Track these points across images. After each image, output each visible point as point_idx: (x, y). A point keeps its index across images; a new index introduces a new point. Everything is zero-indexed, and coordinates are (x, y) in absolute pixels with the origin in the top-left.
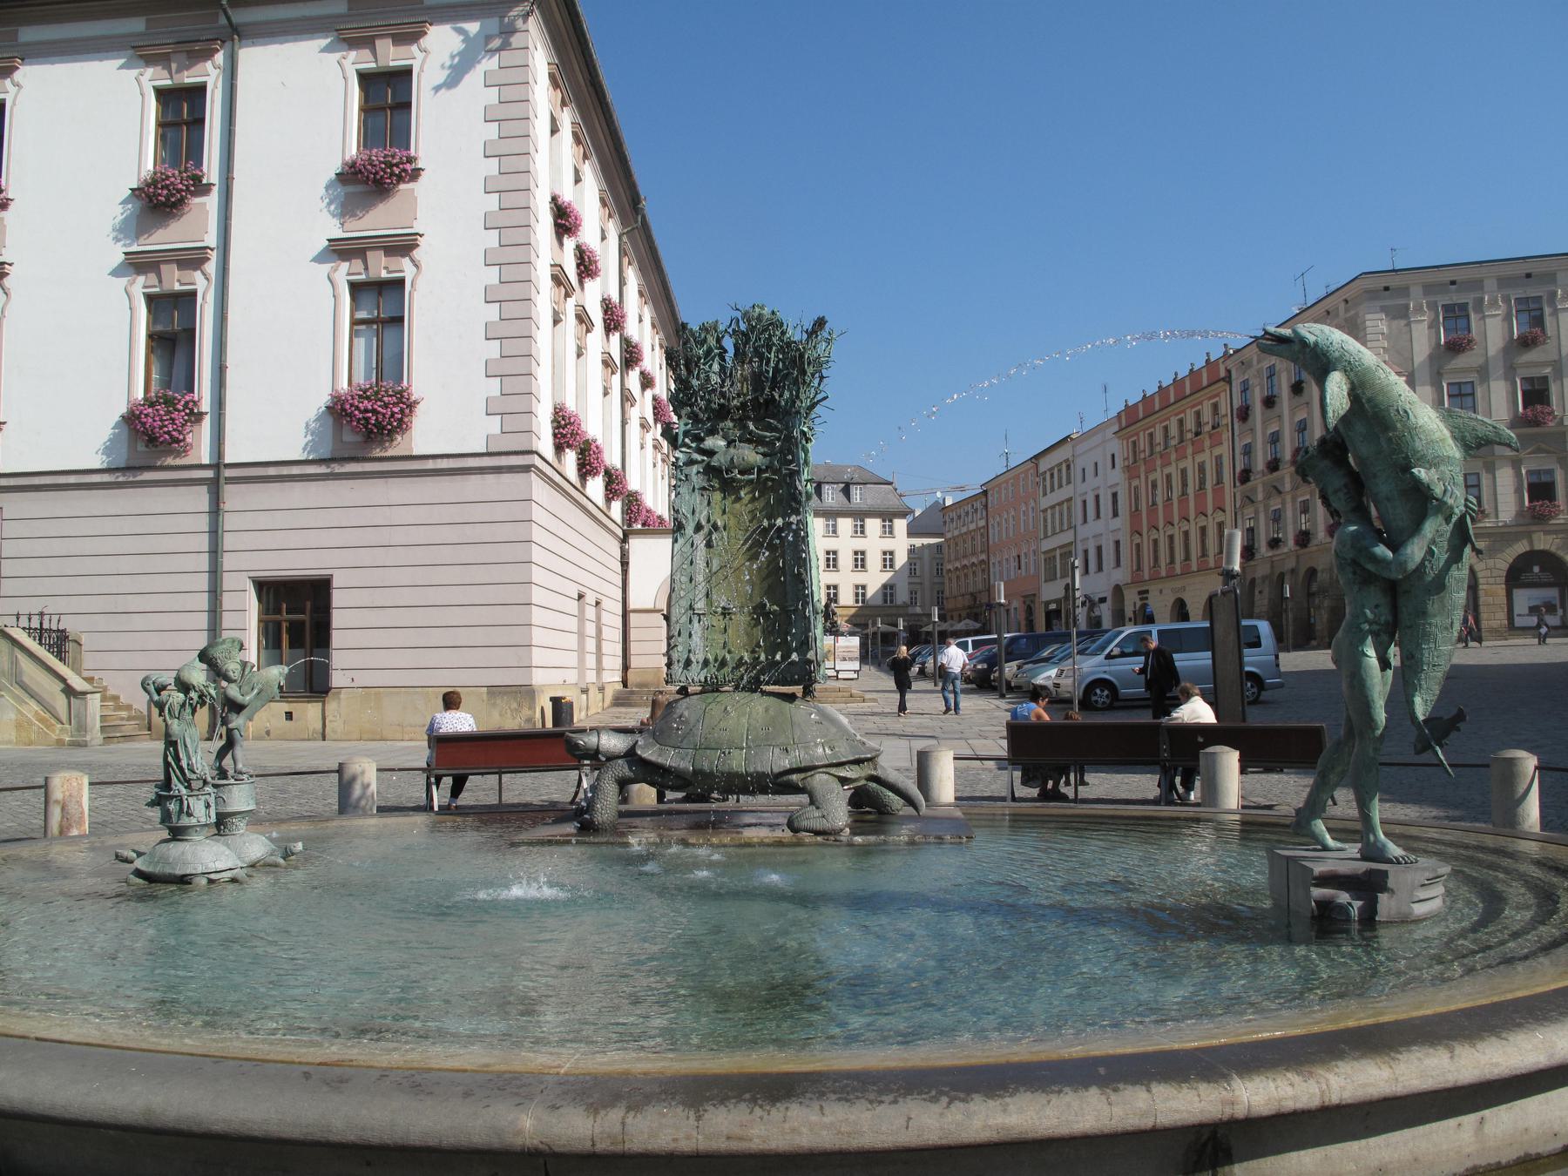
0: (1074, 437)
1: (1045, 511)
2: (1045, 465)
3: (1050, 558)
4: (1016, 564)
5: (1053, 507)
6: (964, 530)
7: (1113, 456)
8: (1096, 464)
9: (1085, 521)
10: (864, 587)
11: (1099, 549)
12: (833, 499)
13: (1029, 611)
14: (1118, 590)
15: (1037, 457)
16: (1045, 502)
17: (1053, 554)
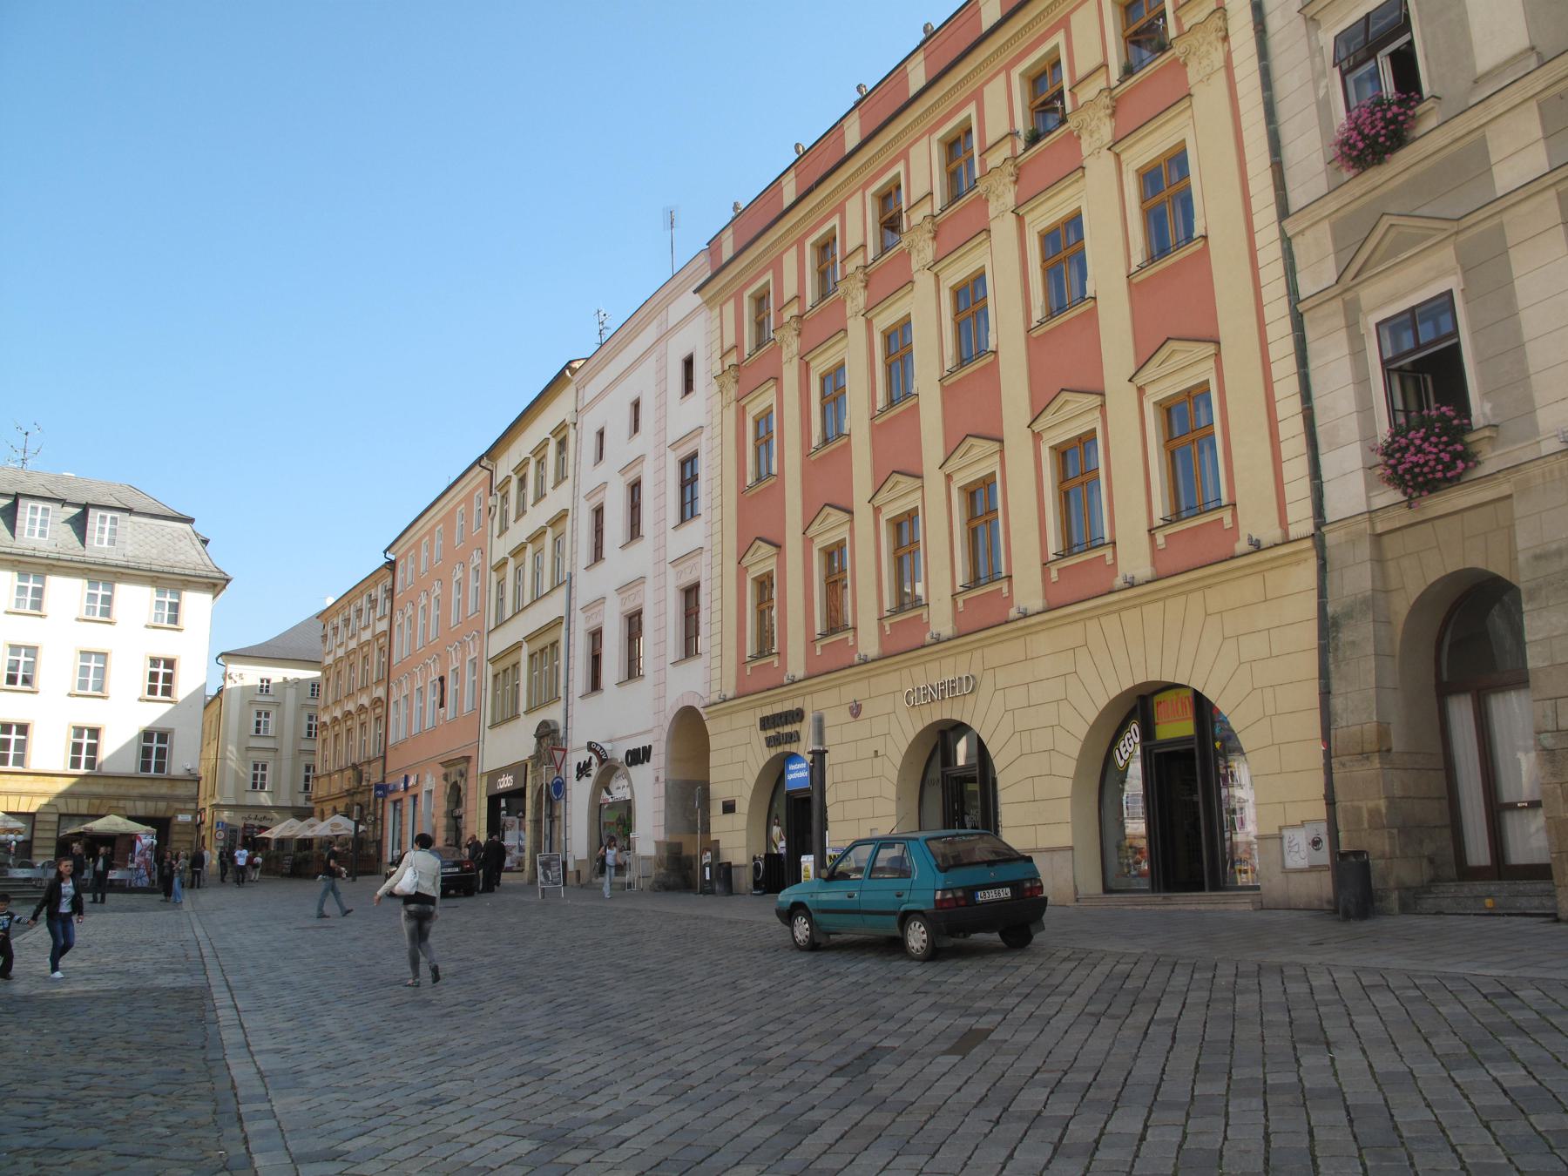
0: (576, 365)
2: (505, 466)
4: (437, 698)
6: (353, 644)
7: (689, 363)
8: (636, 405)
10: (95, 733)
12: (42, 533)
13: (456, 796)
15: (493, 453)
16: (501, 548)
17: (508, 662)
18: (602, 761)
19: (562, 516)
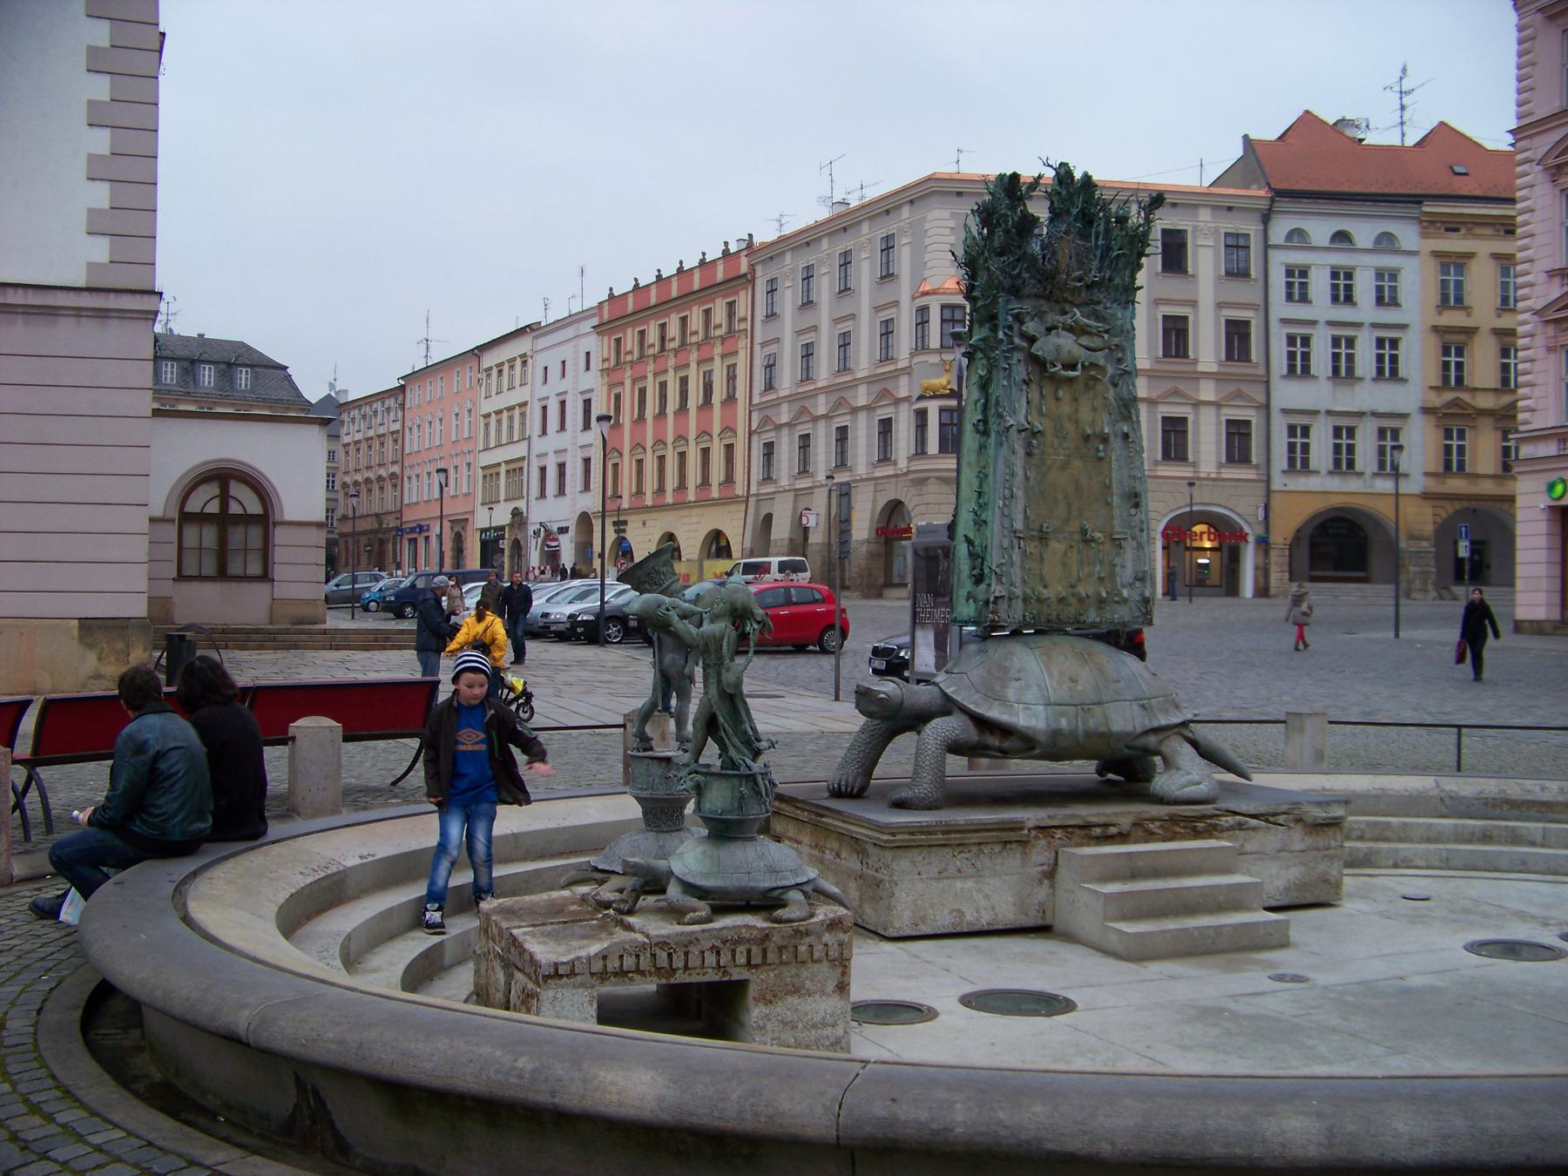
1: (487, 416)
2: (489, 360)
3: (491, 472)
5: (499, 412)
7: (588, 354)
8: (564, 362)
9: (544, 432)
11: (562, 467)
14: (585, 520)
16: (488, 407)
17: (493, 471)
18: (546, 531)
19: (524, 404)
